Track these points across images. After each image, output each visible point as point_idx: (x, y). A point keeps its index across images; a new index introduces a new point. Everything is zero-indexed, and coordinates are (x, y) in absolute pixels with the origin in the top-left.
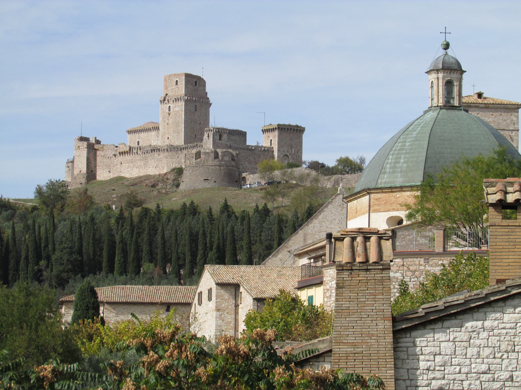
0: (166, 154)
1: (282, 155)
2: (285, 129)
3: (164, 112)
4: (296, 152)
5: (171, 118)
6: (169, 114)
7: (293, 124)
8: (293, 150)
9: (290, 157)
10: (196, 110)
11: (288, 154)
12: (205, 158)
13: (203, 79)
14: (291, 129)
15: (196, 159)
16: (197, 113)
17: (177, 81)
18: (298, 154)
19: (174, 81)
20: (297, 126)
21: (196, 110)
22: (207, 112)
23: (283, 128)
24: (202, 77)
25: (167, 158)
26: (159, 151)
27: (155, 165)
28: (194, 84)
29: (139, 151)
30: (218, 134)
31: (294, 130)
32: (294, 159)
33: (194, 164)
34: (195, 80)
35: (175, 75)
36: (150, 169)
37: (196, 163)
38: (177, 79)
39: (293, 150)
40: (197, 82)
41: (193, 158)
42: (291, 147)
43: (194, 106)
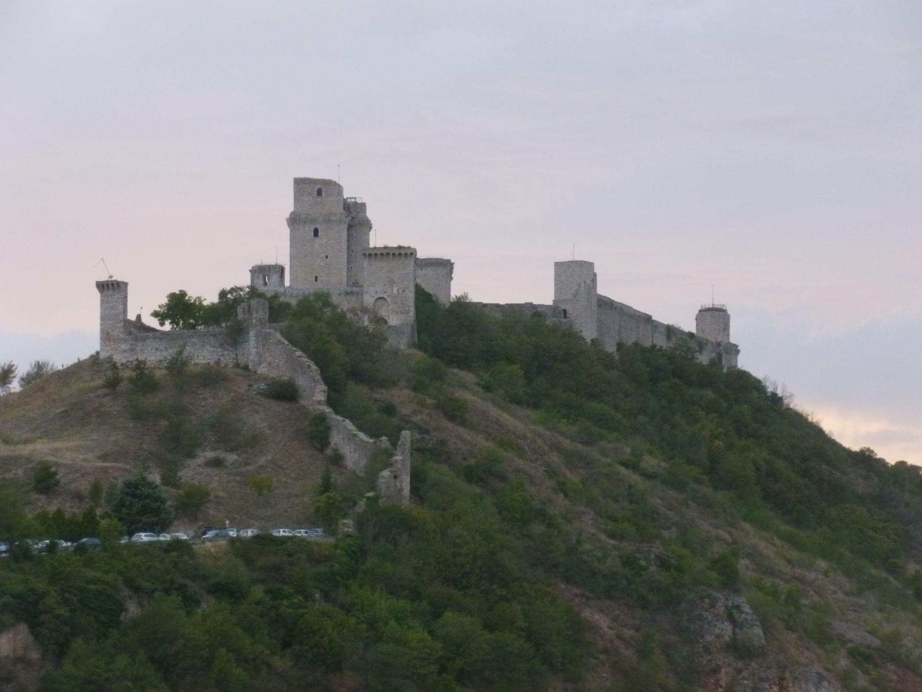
1: (373, 300)
2: (376, 255)
4: (401, 291)
7: (393, 243)
8: (395, 290)
9: (389, 300)
11: (385, 296)
13: (335, 183)
14: (388, 254)
16: (317, 240)
18: (404, 296)
20: (400, 248)
23: (373, 253)
24: (335, 179)
28: (315, 193)
30: (261, 276)
31: (394, 254)
32: (396, 303)
34: (318, 187)
39: (395, 290)
40: (323, 190)
42: (391, 283)
43: (312, 229)
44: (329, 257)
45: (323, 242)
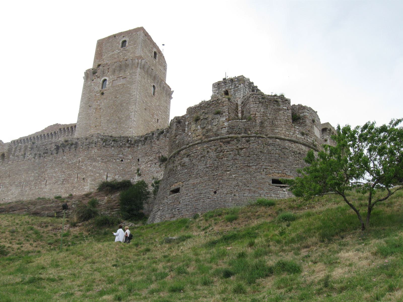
0: (94, 151)
3: (90, 91)
5: (106, 99)
6: (103, 94)
10: (154, 94)
12: (264, 114)
15: (228, 120)
17: (124, 42)
19: (118, 43)
21: (154, 94)
22: (167, 107)
25: (95, 160)
26: (76, 147)
27: (63, 177)
29: (28, 154)
33: (224, 131)
35: (121, 34)
36: (48, 187)
37: (231, 128)
38: (124, 39)
41: (218, 113)
44: (159, 121)
45: (157, 104)
